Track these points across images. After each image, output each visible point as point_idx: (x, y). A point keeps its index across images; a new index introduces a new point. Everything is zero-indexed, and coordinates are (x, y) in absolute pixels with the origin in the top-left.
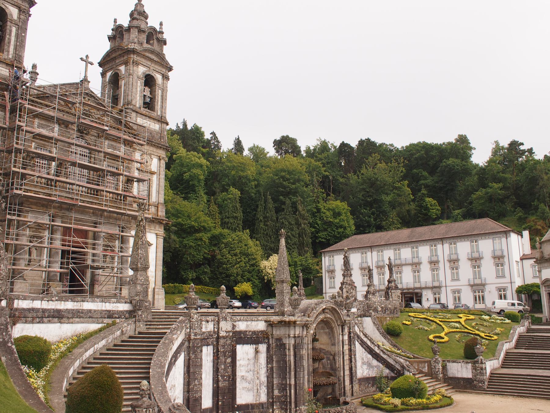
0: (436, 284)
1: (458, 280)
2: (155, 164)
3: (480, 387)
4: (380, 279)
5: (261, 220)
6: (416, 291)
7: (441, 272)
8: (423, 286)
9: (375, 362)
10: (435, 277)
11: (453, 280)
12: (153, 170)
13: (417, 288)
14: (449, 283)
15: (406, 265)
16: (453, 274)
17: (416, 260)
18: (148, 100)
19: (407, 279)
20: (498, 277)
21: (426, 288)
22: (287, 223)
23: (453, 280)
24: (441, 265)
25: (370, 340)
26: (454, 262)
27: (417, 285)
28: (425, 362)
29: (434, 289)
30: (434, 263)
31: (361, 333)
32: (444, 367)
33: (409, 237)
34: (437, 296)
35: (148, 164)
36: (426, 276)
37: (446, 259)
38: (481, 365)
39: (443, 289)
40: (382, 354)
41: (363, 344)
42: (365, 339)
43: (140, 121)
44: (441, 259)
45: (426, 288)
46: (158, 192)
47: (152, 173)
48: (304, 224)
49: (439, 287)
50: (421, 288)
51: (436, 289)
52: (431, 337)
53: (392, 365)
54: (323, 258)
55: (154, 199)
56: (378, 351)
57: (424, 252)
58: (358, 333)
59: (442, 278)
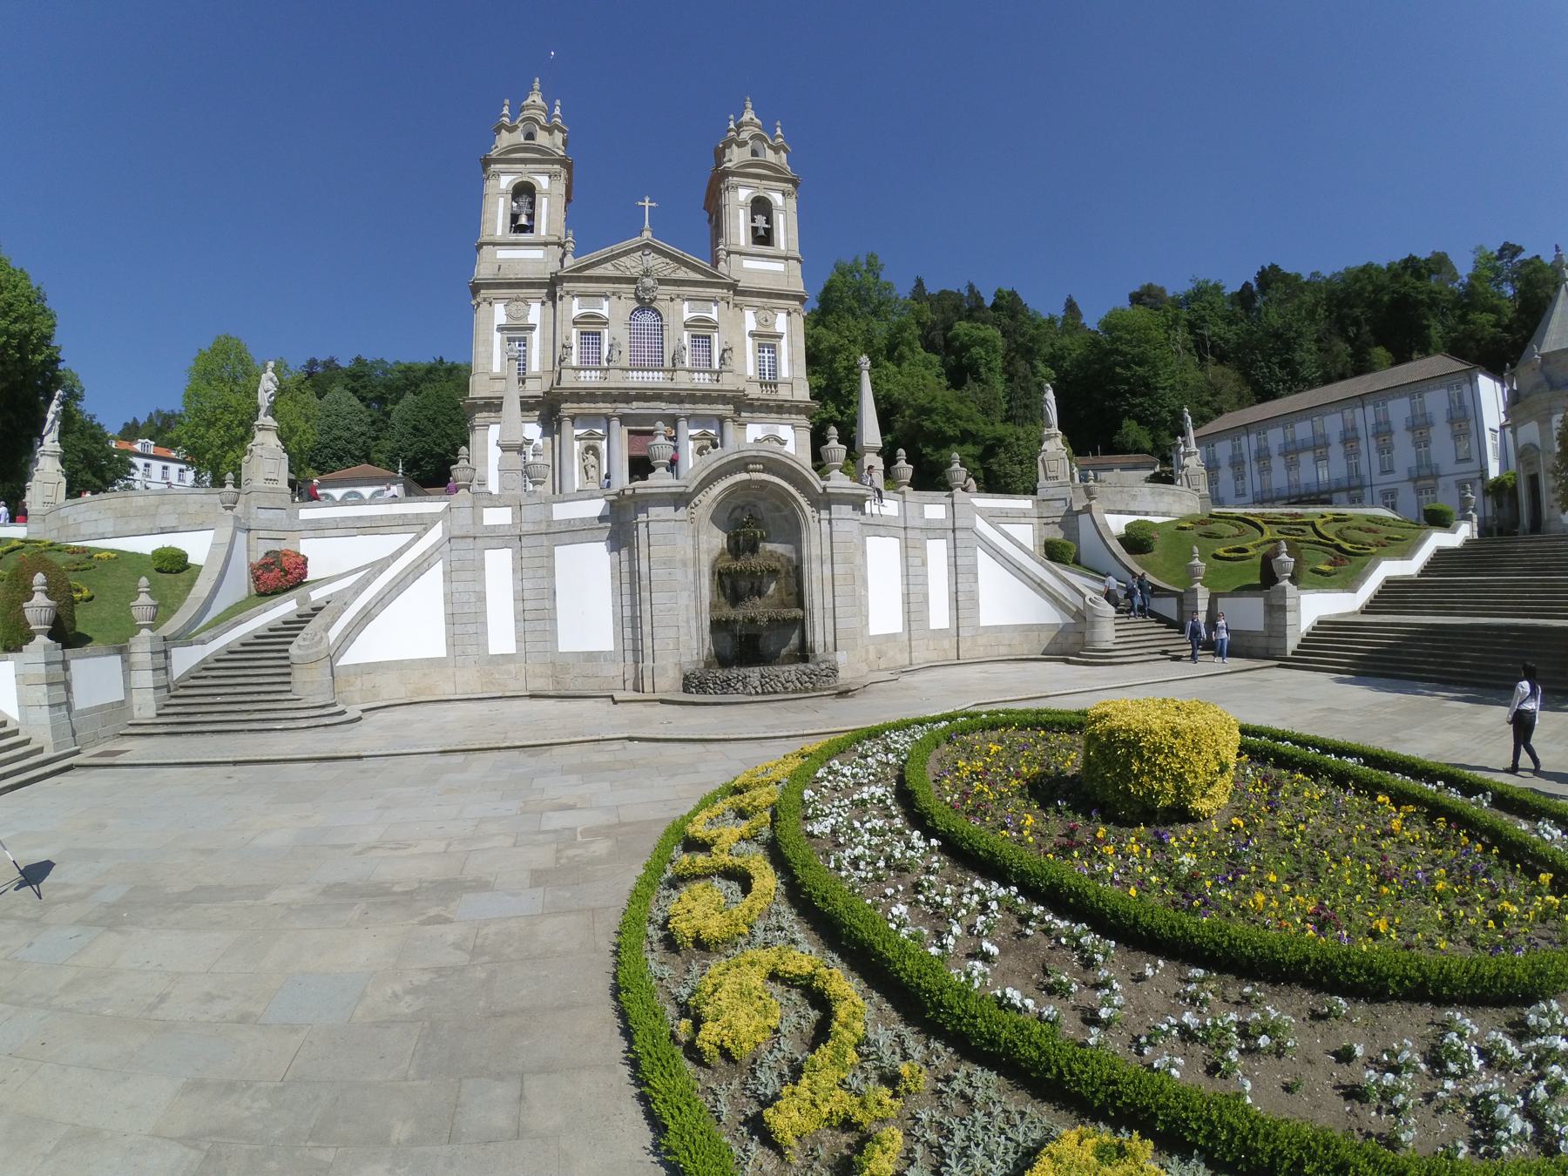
0: (1355, 482)
1: (1391, 471)
2: (781, 323)
8: (1333, 487)
14: (1377, 479)
15: (1305, 449)
18: (762, 233)
20: (1459, 461)
23: (1383, 473)
24: (1362, 446)
39: (1367, 491)
43: (749, 264)
44: (1362, 433)
46: (792, 362)
49: (1361, 487)
50: (1330, 492)
55: (785, 372)
59: (1364, 470)
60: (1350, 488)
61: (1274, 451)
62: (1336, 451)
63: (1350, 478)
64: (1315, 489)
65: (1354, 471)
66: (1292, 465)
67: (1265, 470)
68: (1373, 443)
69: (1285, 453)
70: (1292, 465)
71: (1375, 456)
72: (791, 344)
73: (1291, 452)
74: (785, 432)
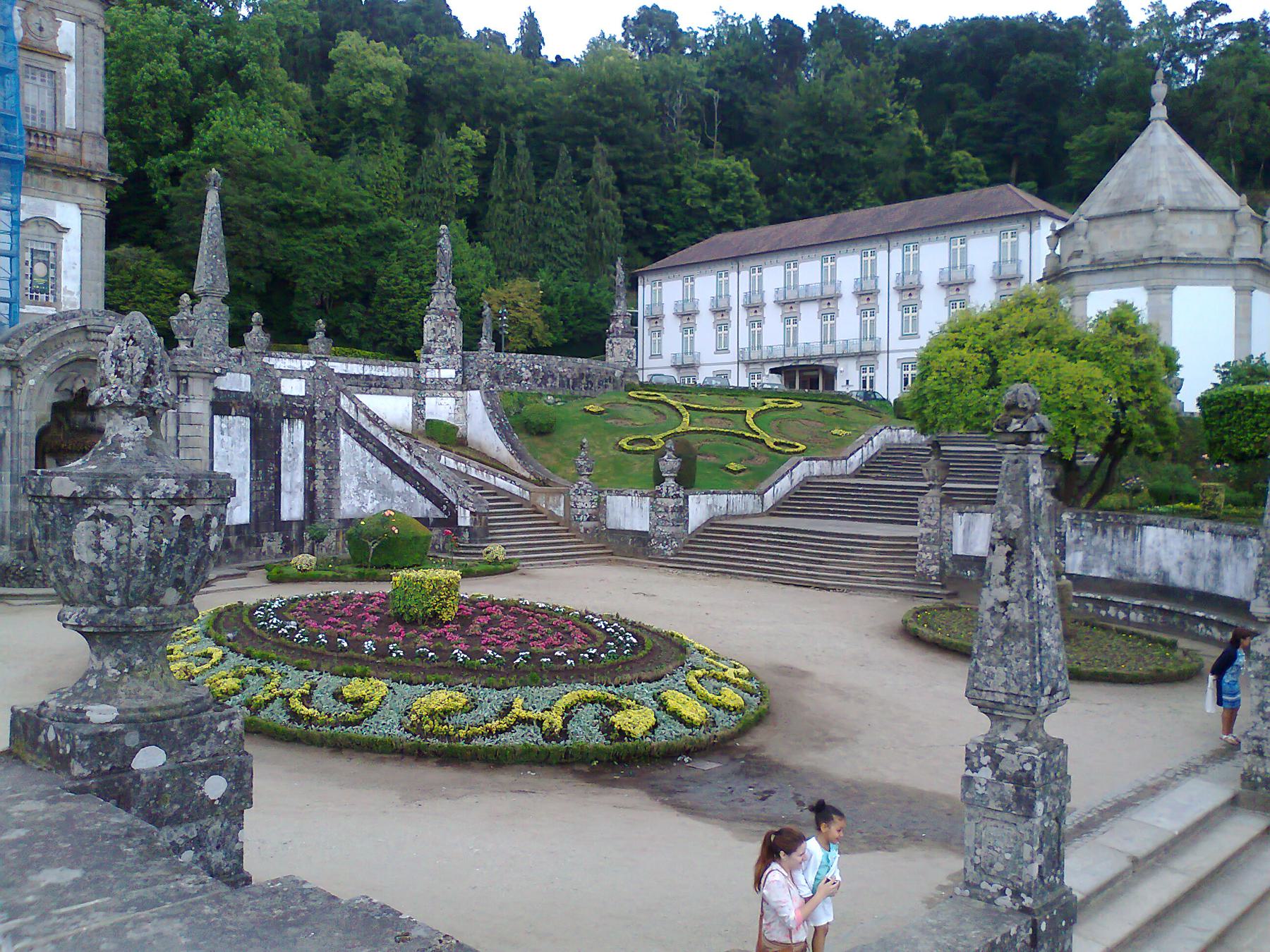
0: (867, 347)
3: (661, 551)
4: (752, 335)
5: (499, 199)
6: (824, 363)
7: (881, 318)
9: (398, 484)
10: (867, 332)
11: (904, 336)
12: (61, 50)
13: (829, 357)
16: (904, 321)
17: (829, 291)
19: (809, 334)
21: (846, 356)
22: (558, 205)
23: (904, 336)
24: (882, 300)
25: (387, 433)
26: (909, 290)
27: (828, 350)
28: (560, 493)
29: (863, 359)
30: (866, 295)
31: (362, 416)
32: (601, 506)
33: (824, 233)
34: (868, 374)
35: (45, 33)
36: (848, 327)
37: (893, 285)
38: (666, 501)
39: (882, 358)
40: (416, 466)
41: (363, 438)
42: (373, 430)
45: (846, 356)
46: (81, 106)
47: (66, 58)
48: (607, 208)
49: (874, 354)
51: (866, 357)
52: (624, 443)
53: (438, 491)
54: (640, 288)
55: (70, 117)
56: (408, 460)
57: (848, 266)
58: (352, 414)
59: (881, 332)
60: (862, 354)
61: (769, 298)
62: (848, 308)
63: (862, 339)
64: (817, 352)
65: (867, 332)
66: (791, 320)
67: (756, 323)
68: (895, 299)
69: (783, 303)
70: (791, 320)
71: (896, 315)
72: (81, 74)
73: (790, 304)
74: (67, 214)
